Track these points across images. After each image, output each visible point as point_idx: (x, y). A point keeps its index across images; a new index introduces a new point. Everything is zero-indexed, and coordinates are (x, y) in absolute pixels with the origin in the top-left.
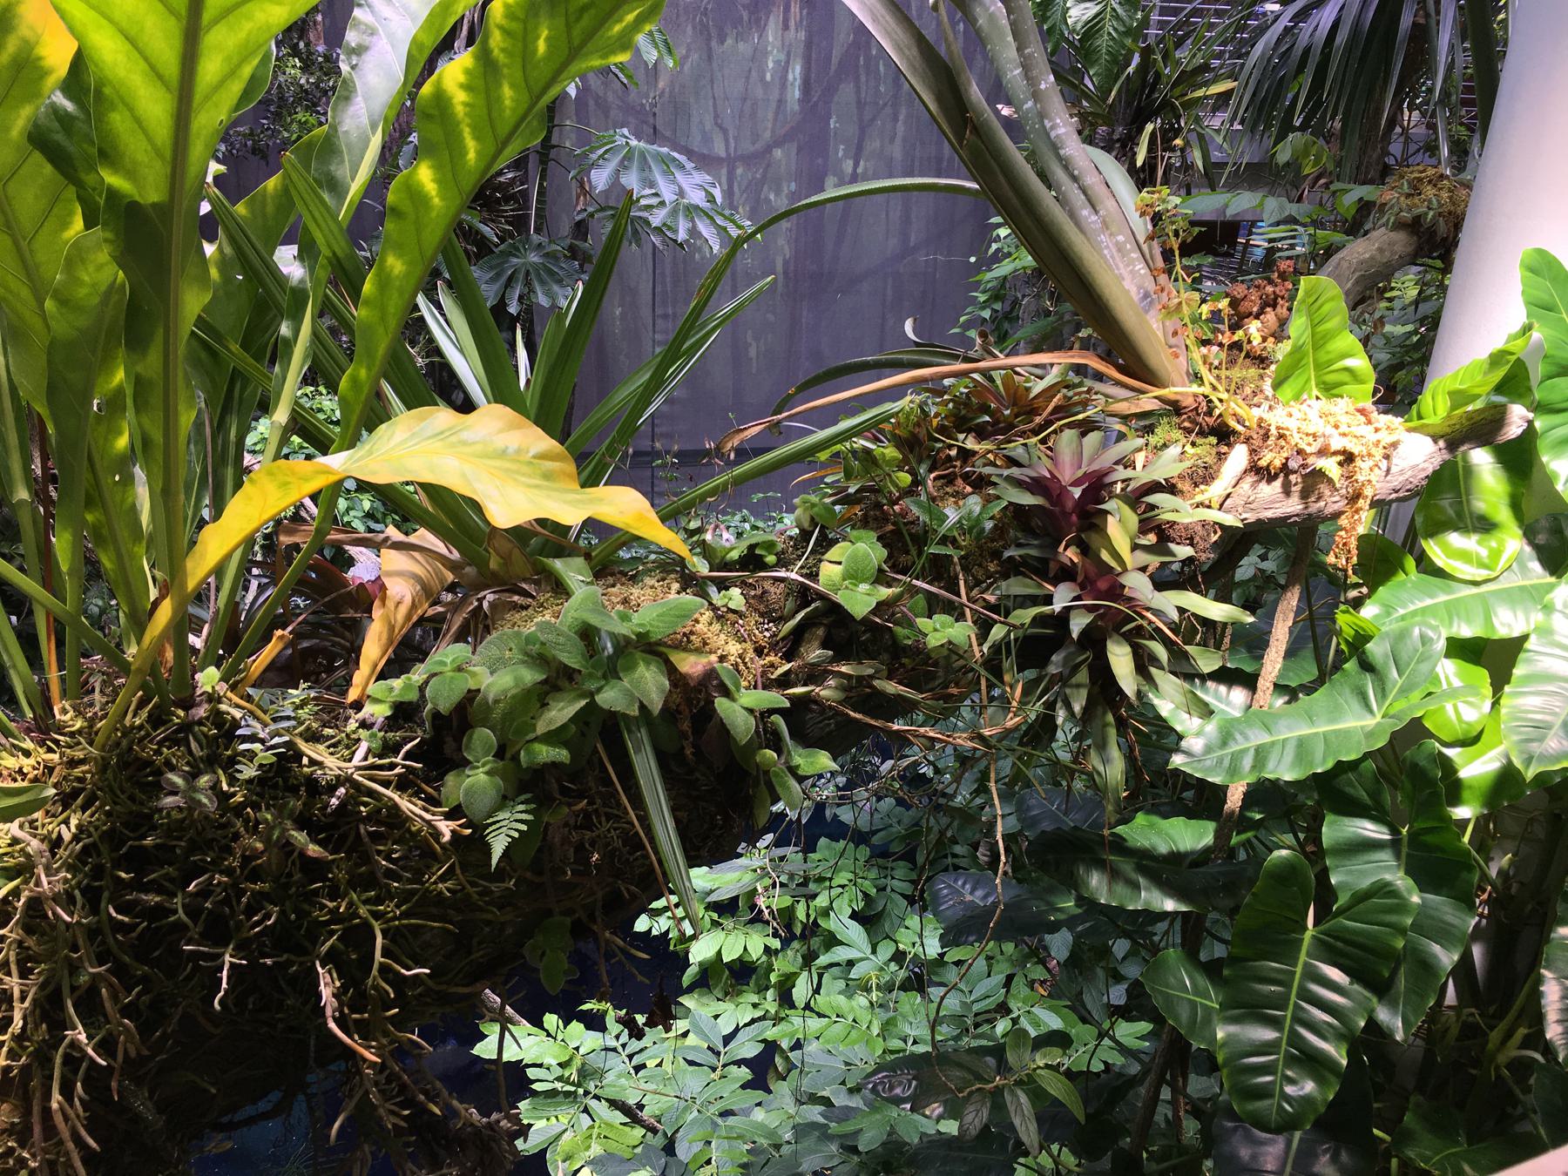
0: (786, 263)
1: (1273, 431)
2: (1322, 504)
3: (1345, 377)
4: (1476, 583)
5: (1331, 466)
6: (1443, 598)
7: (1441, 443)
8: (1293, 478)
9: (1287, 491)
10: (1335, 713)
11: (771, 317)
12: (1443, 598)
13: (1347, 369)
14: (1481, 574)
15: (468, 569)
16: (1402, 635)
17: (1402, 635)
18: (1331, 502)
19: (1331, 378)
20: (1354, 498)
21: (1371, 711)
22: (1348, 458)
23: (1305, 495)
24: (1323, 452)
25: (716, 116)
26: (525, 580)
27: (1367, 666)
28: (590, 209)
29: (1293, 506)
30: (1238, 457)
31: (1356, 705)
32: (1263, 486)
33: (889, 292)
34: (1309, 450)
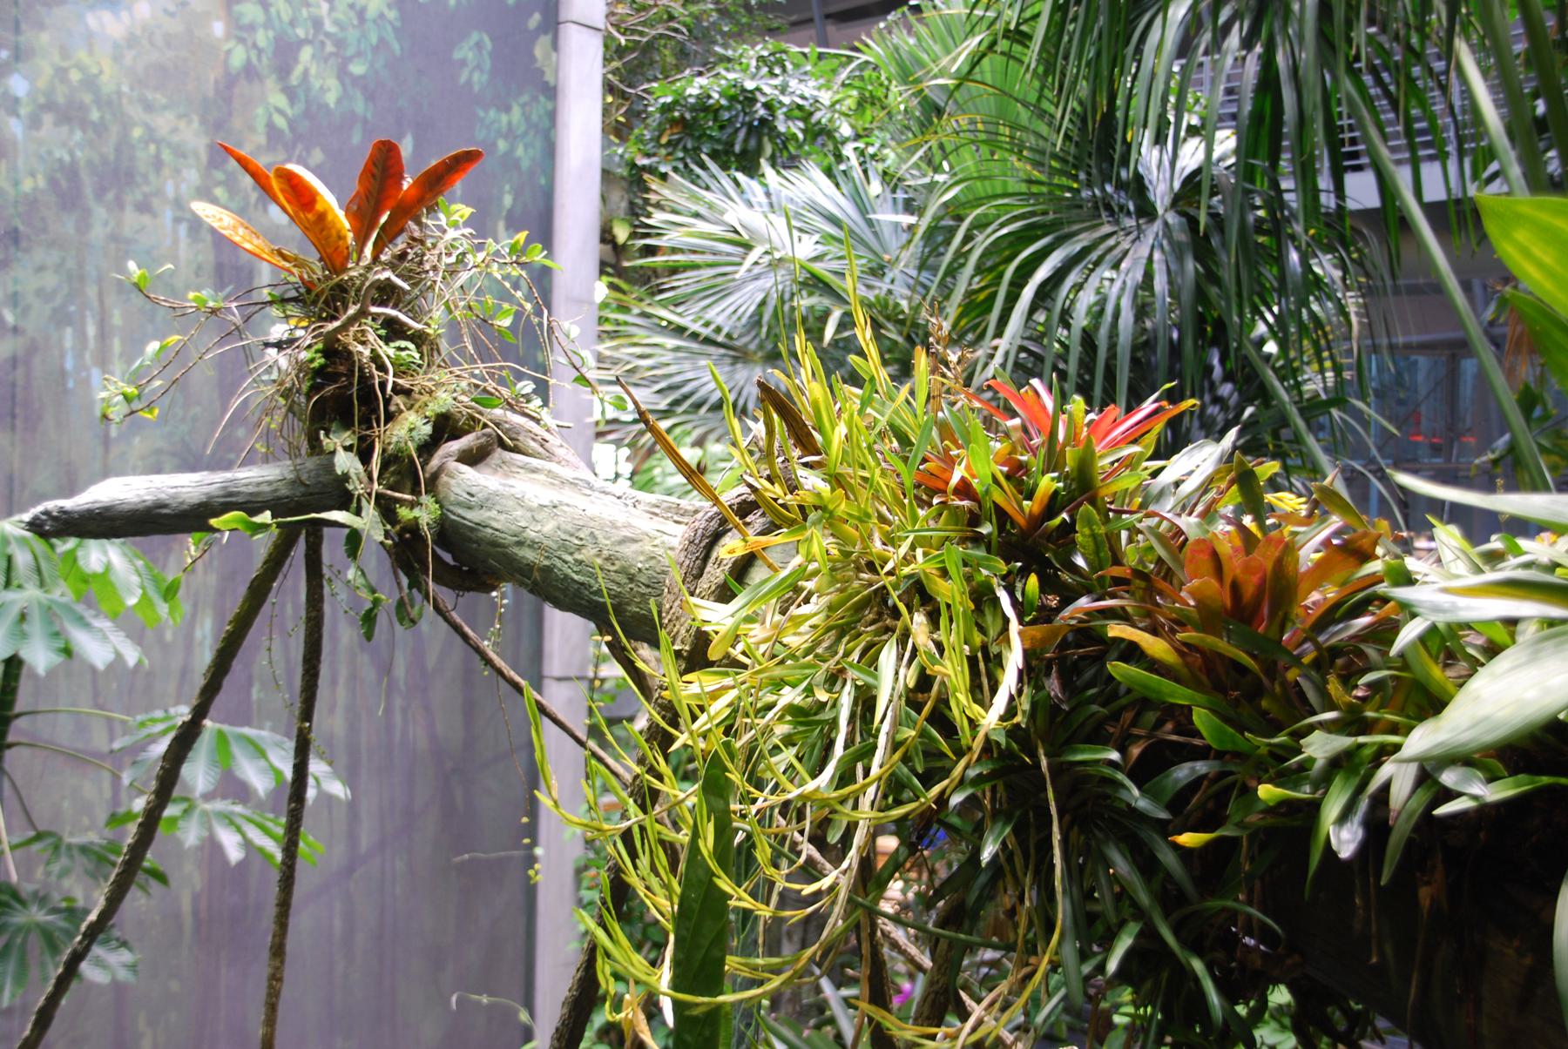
0: (196, 899)
11: (175, 986)
25: (96, 695)
33: (338, 923)
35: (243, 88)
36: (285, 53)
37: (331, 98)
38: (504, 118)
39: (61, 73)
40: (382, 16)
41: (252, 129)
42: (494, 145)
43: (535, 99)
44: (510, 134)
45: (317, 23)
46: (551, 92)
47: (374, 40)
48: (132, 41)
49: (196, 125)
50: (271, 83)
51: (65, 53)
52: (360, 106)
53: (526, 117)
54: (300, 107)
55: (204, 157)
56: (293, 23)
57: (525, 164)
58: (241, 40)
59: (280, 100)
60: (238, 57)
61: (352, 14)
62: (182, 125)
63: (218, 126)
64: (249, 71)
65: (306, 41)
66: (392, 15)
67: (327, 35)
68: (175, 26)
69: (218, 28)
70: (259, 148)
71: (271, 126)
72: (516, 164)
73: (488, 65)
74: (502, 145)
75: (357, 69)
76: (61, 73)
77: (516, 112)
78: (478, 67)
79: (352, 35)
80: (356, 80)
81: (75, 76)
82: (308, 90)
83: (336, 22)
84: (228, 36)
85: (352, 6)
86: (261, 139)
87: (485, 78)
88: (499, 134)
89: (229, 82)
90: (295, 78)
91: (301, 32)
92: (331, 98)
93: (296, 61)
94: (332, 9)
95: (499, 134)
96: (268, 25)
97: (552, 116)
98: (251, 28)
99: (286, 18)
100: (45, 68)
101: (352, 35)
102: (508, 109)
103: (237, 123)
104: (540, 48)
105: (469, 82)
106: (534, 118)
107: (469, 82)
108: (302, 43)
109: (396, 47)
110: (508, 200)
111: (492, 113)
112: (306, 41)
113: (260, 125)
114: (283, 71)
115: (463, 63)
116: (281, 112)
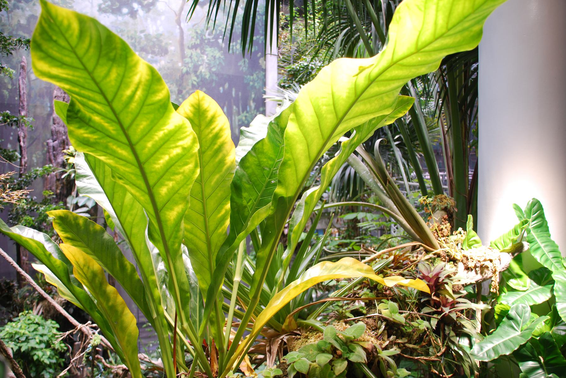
1: (469, 258)
2: (486, 275)
3: (474, 242)
4: (525, 291)
5: (488, 263)
6: (519, 297)
7: (510, 254)
8: (477, 269)
9: (477, 274)
10: (507, 334)
12: (519, 297)
13: (475, 240)
14: (525, 289)
15: (269, 331)
16: (517, 308)
17: (517, 308)
18: (488, 274)
19: (470, 243)
20: (494, 272)
21: (516, 330)
22: (491, 261)
23: (481, 273)
24: (485, 260)
26: (295, 330)
27: (510, 318)
28: (119, 241)
29: (479, 277)
30: (461, 266)
31: (510, 330)
32: (470, 272)
34: (481, 260)
35: (186, 76)
37: (207, 77)
38: (252, 77)
40: (220, 57)
41: (188, 85)
42: (249, 84)
43: (260, 72)
44: (253, 81)
46: (265, 70)
47: (218, 63)
49: (175, 85)
52: (215, 78)
53: (258, 77)
54: (200, 79)
55: (177, 92)
56: (198, 61)
57: (257, 87)
58: (185, 66)
59: (195, 78)
60: (185, 70)
61: (212, 58)
62: (171, 86)
63: (180, 85)
64: (187, 73)
65: (201, 65)
66: (222, 57)
68: (170, 65)
69: (180, 64)
70: (190, 89)
72: (255, 88)
73: (247, 66)
74: (251, 83)
75: (214, 70)
77: (255, 76)
78: (245, 66)
79: (212, 62)
80: (214, 73)
82: (202, 75)
83: (208, 60)
84: (182, 66)
86: (190, 87)
87: (246, 69)
88: (250, 81)
89: (182, 76)
90: (198, 73)
91: (200, 63)
92: (207, 77)
93: (199, 69)
94: (207, 57)
95: (250, 81)
96: (192, 62)
97: (265, 76)
98: (188, 63)
99: (196, 60)
101: (212, 62)
102: (252, 75)
103: (184, 84)
104: (261, 61)
105: (242, 70)
106: (260, 76)
107: (242, 70)
109: (224, 64)
110: (253, 96)
111: (249, 76)
112: (201, 65)
113: (190, 84)
114: (195, 72)
115: (241, 66)
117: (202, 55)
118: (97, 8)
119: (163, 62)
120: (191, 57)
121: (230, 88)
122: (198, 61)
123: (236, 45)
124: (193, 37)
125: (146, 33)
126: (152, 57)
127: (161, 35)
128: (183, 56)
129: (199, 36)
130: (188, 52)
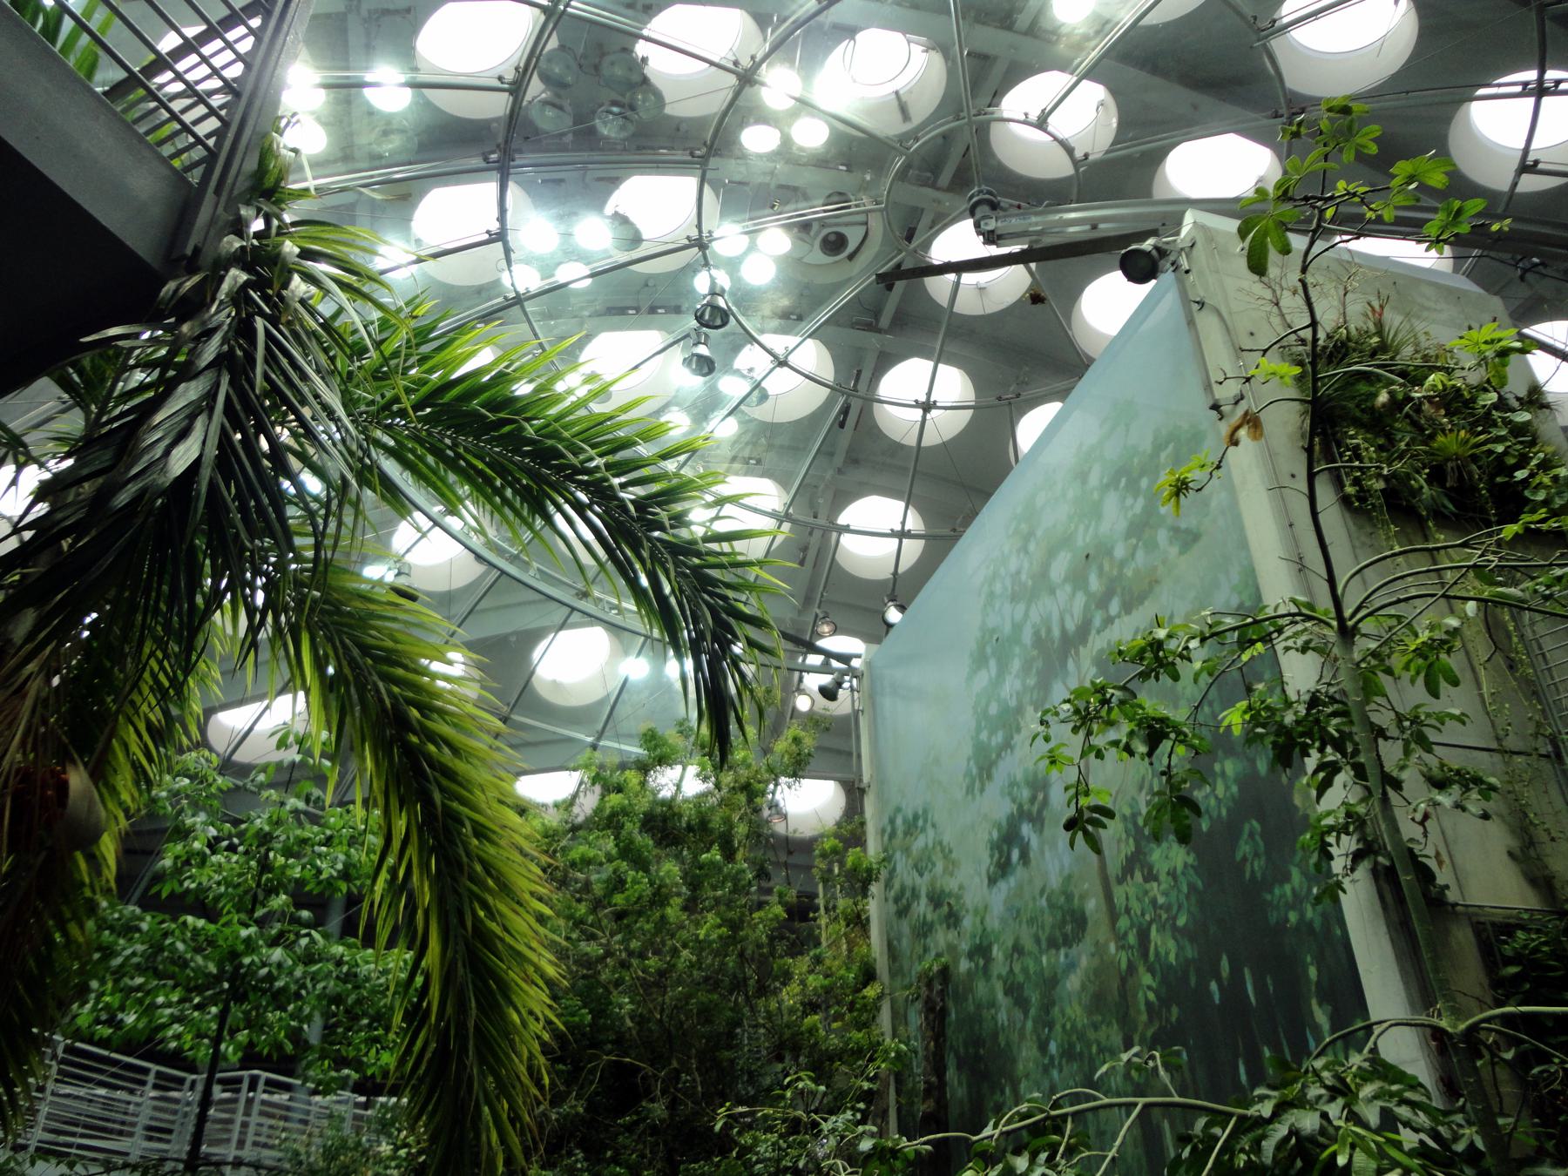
36: (1144, 936)
39: (1064, 1026)
40: (1186, 865)
45: (1154, 902)
47: (1185, 889)
48: (1084, 987)
50: (1141, 969)
51: (1063, 1012)
56: (1143, 915)
58: (1123, 947)
60: (1124, 965)
64: (1131, 968)
66: (1191, 859)
67: (1161, 907)
69: (1112, 947)
71: (1148, 1003)
76: (1064, 1026)
81: (1068, 1026)
85: (1168, 873)
89: (1123, 980)
92: (1172, 958)
100: (1058, 1028)
103: (1132, 1012)
107: (1253, 872)
108: (1150, 923)
109: (1200, 884)
113: (1143, 1007)
114: (1145, 954)
116: (1149, 988)
117: (1148, 886)
118: (986, 881)
119: (1084, 961)
120: (1128, 910)
121: (1236, 971)
122: (1143, 915)
123: (1214, 790)
124: (1119, 841)
125: (1048, 891)
126: (1066, 956)
127: (1069, 877)
128: (1114, 916)
129: (1130, 826)
130: (1119, 893)
